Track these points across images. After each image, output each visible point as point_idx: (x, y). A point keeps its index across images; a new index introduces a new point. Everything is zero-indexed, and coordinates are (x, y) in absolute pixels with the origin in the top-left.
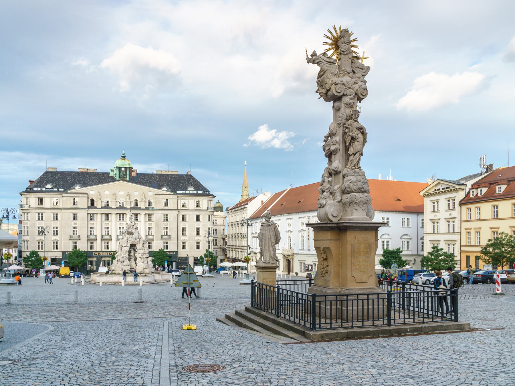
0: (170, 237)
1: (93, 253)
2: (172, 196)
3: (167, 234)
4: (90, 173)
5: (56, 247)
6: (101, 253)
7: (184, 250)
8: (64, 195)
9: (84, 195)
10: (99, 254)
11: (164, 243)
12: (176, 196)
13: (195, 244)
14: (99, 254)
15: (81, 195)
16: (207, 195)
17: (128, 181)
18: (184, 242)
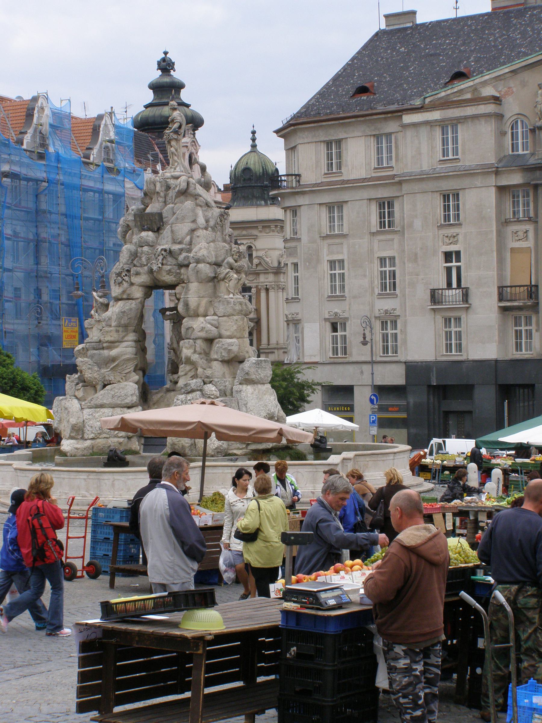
8: (408, 119)
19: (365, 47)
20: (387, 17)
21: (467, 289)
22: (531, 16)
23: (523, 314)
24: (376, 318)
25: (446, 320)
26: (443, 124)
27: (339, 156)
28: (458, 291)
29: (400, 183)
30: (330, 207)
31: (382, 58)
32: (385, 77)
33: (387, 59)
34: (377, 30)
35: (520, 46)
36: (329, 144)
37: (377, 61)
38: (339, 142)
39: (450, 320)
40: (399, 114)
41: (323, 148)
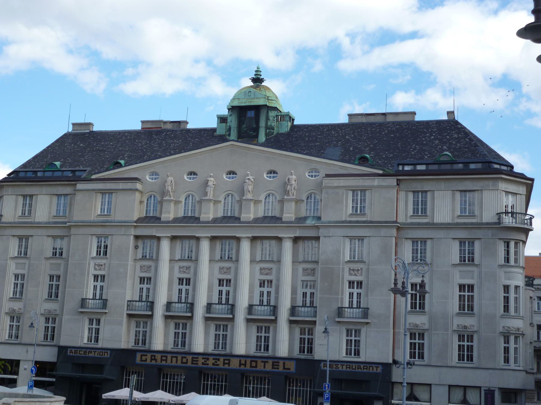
0: (366, 313)
1: (138, 355)
2: (376, 182)
3: (359, 303)
4: (168, 131)
5: (51, 334)
6: (158, 356)
7: (417, 361)
9: (129, 185)
10: (153, 358)
11: (349, 332)
12: (393, 181)
13: (456, 343)
14: (153, 358)
15: (121, 185)
16: (499, 172)
17: (262, 145)
18: (418, 334)
19: (57, 141)
20: (74, 124)
21: (107, 300)
22: (166, 135)
23: (142, 320)
24: (42, 314)
25: (90, 320)
26: (103, 192)
27: (30, 205)
28: (100, 301)
29: (69, 227)
30: (20, 238)
31: (67, 149)
32: (68, 160)
33: (71, 150)
34: (66, 132)
35: (158, 151)
36: (24, 196)
37: (64, 150)
38: (31, 196)
39: (93, 320)
40: (75, 183)
41: (21, 199)
